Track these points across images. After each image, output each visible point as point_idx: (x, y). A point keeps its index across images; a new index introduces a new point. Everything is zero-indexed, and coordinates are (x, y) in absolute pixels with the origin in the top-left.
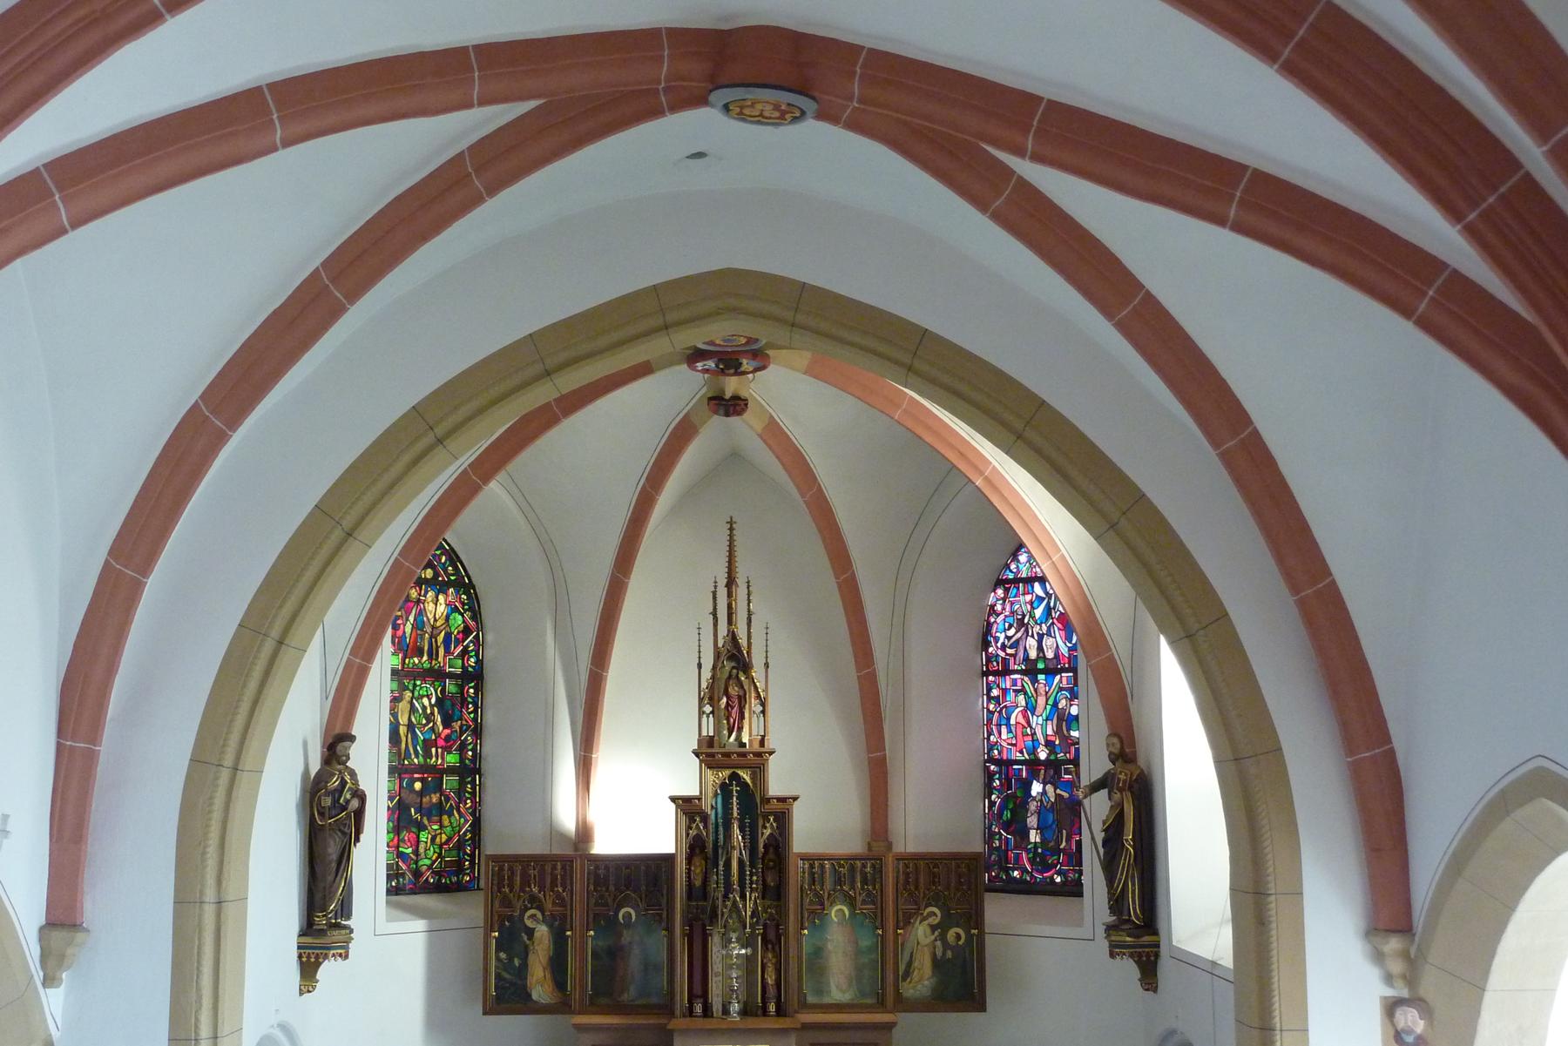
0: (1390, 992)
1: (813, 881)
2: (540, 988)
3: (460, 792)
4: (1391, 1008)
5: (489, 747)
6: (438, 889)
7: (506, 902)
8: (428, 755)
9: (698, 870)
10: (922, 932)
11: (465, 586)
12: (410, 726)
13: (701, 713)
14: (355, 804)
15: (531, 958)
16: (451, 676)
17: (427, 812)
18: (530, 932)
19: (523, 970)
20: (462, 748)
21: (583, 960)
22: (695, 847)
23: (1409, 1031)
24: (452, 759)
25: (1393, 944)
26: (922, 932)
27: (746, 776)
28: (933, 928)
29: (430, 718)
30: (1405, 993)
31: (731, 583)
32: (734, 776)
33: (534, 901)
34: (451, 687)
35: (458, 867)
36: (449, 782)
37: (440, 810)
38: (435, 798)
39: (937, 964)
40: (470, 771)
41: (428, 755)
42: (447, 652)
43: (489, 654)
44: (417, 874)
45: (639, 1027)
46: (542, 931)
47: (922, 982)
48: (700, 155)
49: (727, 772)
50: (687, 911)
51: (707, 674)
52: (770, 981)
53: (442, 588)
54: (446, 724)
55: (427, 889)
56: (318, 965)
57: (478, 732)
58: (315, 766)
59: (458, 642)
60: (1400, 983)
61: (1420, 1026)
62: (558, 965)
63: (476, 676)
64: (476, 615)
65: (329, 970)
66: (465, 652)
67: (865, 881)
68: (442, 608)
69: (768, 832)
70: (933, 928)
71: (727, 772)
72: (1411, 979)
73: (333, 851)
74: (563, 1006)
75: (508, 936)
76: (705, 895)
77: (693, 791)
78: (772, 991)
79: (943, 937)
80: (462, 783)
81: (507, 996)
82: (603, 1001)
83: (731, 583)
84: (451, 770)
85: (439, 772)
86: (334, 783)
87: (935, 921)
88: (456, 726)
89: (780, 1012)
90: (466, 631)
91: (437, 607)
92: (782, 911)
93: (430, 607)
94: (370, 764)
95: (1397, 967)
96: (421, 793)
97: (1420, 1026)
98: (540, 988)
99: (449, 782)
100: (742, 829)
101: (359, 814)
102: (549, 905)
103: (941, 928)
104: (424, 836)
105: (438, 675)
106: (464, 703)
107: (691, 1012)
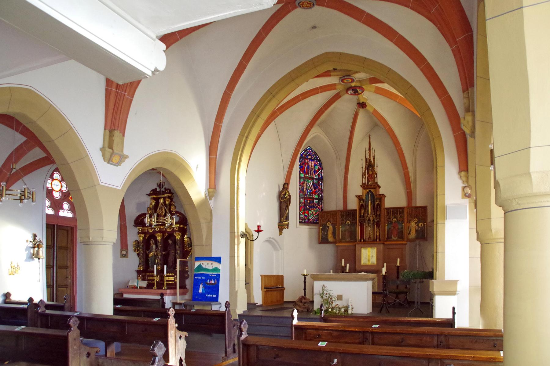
0: (464, 185)
1: (388, 214)
2: (330, 238)
3: (318, 203)
4: (464, 188)
5: (325, 195)
6: (314, 223)
7: (323, 221)
8: (310, 195)
9: (363, 211)
10: (413, 224)
11: (318, 160)
12: (306, 189)
13: (363, 178)
14: (288, 197)
15: (329, 233)
16: (316, 179)
17: (311, 207)
18: (328, 227)
19: (327, 234)
20: (318, 194)
21: (339, 234)
22: (362, 207)
23: (467, 193)
24: (316, 196)
25: (463, 173)
26: (413, 224)
27: (372, 190)
28: (416, 223)
29: (311, 188)
30: (467, 185)
31: (370, 149)
32: (370, 191)
33: (329, 221)
34: (315, 181)
35: (317, 219)
36: (316, 201)
37: (313, 207)
38: (312, 204)
39: (416, 231)
40: (320, 199)
41: (310, 195)
42: (315, 174)
43: (324, 175)
44: (309, 220)
45: (350, 246)
46: (331, 227)
47: (413, 235)
48: (314, 27)
49: (368, 191)
50: (360, 220)
51: (364, 169)
52: (378, 235)
53: (313, 160)
54: (315, 189)
55: (311, 223)
56: (283, 229)
57: (322, 191)
58: (281, 189)
59: (317, 172)
60: (465, 183)
61: (469, 192)
62: (334, 233)
63: (322, 179)
64: (321, 166)
65: (285, 231)
66: (319, 174)
67: (400, 213)
68: (313, 164)
69: (377, 203)
70: (416, 223)
71: (368, 191)
72: (468, 182)
73: (284, 207)
74: (335, 242)
75: (325, 228)
76: (364, 217)
77: (360, 193)
78: (378, 237)
79: (418, 225)
80: (319, 202)
81: (323, 240)
82: (343, 241)
83: (370, 149)
84: (316, 199)
85: (314, 199)
86: (284, 193)
87: (416, 221)
88: (317, 189)
89: (380, 240)
90: (319, 170)
91: (312, 164)
92: (380, 219)
93: (310, 164)
94: (294, 191)
95: (464, 179)
96: (309, 203)
97: (469, 192)
98: (330, 238)
99: (316, 201)
100: (371, 202)
101: (289, 200)
102: (332, 221)
103: (417, 223)
104: (310, 212)
105: (313, 179)
106: (319, 185)
107: (361, 241)
